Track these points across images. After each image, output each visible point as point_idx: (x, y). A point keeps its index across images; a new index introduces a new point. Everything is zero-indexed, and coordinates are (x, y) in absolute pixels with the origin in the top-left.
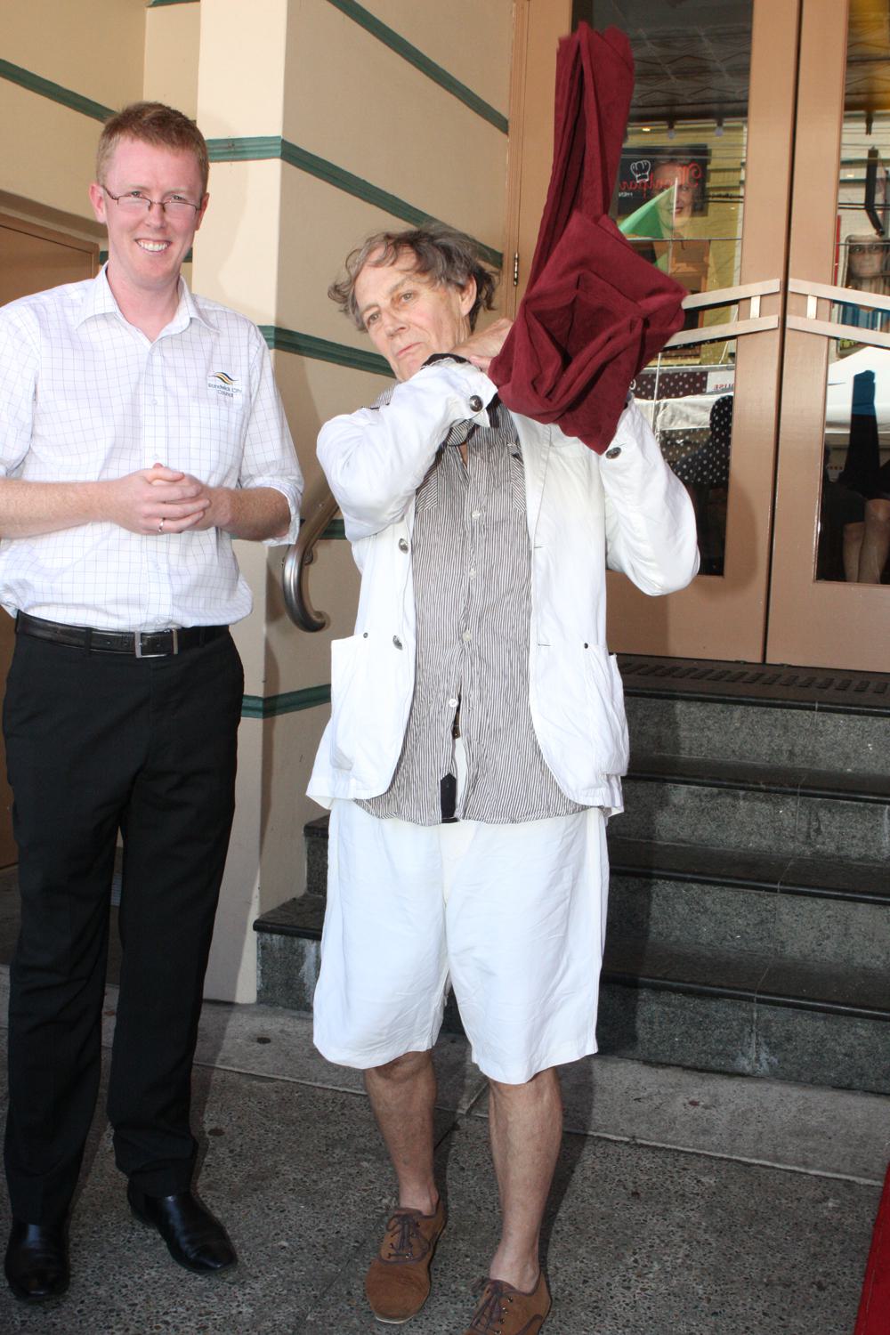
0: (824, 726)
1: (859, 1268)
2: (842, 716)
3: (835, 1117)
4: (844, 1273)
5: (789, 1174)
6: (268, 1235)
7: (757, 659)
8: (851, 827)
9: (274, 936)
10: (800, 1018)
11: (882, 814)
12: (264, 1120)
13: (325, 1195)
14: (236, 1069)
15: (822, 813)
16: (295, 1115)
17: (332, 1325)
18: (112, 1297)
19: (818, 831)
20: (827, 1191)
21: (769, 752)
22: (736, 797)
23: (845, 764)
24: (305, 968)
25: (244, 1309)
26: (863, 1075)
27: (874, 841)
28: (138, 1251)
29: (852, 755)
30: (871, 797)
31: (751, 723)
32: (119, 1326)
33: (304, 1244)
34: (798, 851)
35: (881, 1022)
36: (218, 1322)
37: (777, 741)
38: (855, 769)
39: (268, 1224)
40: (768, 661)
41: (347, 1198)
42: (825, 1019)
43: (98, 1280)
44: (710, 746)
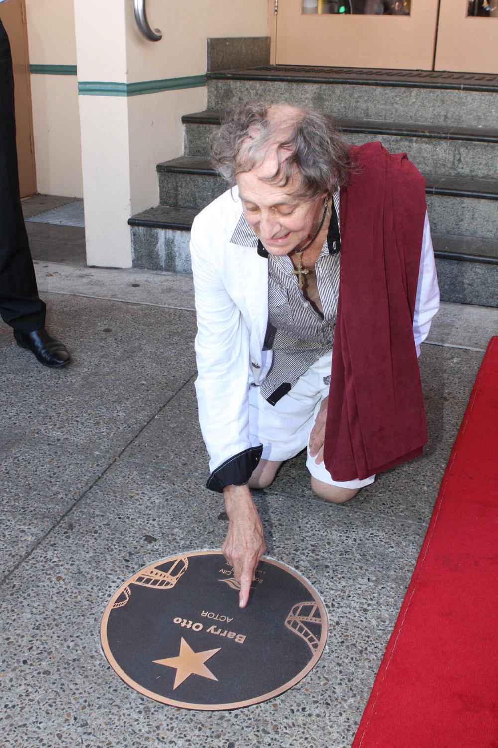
1: (468, 391)
2: (477, 93)
5: (432, 346)
7: (430, 69)
8: (479, 158)
9: (140, 228)
10: (443, 264)
12: (135, 324)
13: (168, 359)
14: (120, 300)
16: (152, 321)
17: (169, 420)
18: (47, 410)
19: (459, 160)
20: (453, 354)
21: (433, 117)
23: (478, 123)
24: (159, 245)
25: (120, 414)
26: (478, 296)
27: (492, 166)
29: (483, 117)
30: (492, 139)
31: (422, 99)
32: (51, 424)
33: (155, 382)
34: (447, 173)
36: (106, 420)
37: (438, 110)
38: (483, 126)
39: (135, 373)
40: (436, 69)
42: (458, 264)
43: (40, 402)
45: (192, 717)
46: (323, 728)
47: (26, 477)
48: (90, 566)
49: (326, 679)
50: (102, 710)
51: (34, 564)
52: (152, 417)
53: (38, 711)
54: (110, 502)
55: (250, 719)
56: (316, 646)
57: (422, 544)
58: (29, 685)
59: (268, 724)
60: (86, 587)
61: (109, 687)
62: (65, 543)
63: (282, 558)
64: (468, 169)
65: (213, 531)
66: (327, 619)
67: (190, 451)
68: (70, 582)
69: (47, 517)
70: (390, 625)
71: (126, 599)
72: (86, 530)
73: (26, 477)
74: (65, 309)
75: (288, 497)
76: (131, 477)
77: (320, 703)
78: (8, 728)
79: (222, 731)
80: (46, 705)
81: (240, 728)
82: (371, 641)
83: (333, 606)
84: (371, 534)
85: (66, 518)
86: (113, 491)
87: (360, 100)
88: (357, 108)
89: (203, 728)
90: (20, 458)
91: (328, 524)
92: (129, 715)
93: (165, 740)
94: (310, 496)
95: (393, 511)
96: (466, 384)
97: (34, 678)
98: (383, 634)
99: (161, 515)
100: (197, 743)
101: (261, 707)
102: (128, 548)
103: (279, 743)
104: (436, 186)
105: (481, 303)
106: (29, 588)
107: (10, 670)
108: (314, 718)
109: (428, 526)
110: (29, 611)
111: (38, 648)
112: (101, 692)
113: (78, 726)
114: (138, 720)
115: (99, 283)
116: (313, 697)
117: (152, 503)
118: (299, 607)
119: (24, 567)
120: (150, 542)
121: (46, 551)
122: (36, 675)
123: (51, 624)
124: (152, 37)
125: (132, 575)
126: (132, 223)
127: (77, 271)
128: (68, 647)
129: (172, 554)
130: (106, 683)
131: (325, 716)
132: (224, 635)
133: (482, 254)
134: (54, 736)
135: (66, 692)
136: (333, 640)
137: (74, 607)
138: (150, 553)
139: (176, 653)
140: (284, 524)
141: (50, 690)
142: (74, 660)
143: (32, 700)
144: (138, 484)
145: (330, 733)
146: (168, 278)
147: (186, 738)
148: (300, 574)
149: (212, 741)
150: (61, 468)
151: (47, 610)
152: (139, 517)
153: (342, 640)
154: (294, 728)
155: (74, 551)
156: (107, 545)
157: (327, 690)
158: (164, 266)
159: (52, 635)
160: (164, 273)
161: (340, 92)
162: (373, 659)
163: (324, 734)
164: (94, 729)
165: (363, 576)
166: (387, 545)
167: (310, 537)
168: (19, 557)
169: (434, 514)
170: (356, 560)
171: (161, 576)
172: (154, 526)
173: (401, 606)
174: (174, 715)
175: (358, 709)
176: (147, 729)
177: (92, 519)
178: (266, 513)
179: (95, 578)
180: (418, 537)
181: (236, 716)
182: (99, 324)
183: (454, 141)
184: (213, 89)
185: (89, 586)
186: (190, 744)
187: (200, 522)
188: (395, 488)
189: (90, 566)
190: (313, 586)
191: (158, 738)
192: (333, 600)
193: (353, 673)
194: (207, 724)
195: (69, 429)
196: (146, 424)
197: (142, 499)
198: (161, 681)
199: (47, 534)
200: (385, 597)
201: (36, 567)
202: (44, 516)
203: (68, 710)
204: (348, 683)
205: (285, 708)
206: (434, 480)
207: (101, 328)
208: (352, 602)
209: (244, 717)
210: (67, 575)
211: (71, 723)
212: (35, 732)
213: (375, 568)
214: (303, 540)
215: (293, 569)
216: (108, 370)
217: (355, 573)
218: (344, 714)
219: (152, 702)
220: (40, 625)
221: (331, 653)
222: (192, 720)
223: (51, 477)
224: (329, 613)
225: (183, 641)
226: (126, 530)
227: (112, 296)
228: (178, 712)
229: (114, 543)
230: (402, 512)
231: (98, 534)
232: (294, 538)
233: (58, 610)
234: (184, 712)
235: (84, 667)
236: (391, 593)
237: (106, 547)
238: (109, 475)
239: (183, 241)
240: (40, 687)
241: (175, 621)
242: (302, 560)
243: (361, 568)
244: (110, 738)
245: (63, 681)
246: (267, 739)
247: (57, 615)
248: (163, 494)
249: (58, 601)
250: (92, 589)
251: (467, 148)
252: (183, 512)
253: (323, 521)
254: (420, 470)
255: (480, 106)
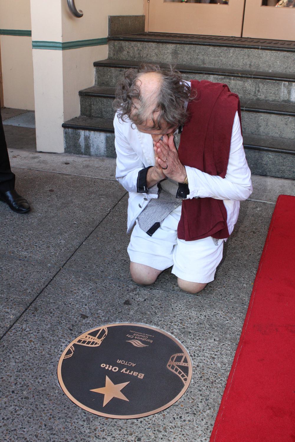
0: (262, 55)
1: (267, 228)
2: (269, 51)
3: (260, 184)
4: (262, 229)
6: (70, 220)
7: (240, 36)
9: (69, 129)
11: (281, 85)
13: (89, 208)
14: (58, 172)
15: (260, 85)
16: (78, 185)
17: (91, 245)
19: (259, 91)
20: (257, 205)
22: (230, 79)
23: (269, 69)
24: (80, 139)
26: (270, 171)
27: (278, 94)
28: (26, 226)
30: (278, 79)
31: (237, 54)
33: (82, 222)
34: (251, 98)
35: (278, 153)
36: (54, 245)
37: (246, 61)
38: (272, 71)
40: (243, 36)
41: (96, 209)
42: (258, 152)
44: (222, 63)
45: (115, 423)
46: (193, 428)
47: (7, 280)
48: (49, 333)
49: (193, 399)
50: (61, 420)
51: (15, 333)
52: (81, 243)
53: (23, 421)
54: (59, 295)
55: (150, 424)
56: (186, 380)
57: (245, 318)
58: (16, 406)
59: (160, 426)
60: (47, 346)
61: (65, 406)
62: (33, 320)
63: (163, 328)
64: (263, 96)
65: (121, 312)
66: (191, 364)
67: (105, 264)
68: (37, 343)
69: (22, 304)
70: (229, 367)
71: (72, 353)
72: (45, 312)
73: (7, 280)
74: (25, 178)
75: (164, 291)
76: (71, 279)
77: (190, 414)
78: (5, 432)
79: (133, 431)
80: (27, 418)
81: (144, 429)
82: (218, 376)
83: (194, 355)
84: (215, 313)
85: (33, 305)
86: (60, 288)
87: (200, 55)
88: (198, 59)
89: (122, 430)
90: (3, 268)
91: (189, 307)
92: (78, 423)
93: (100, 437)
94: (178, 290)
95: (227, 299)
96: (265, 223)
97: (19, 402)
98: (225, 372)
99: (90, 303)
100: (119, 439)
101: (155, 416)
102: (71, 322)
103: (167, 438)
104: (246, 106)
105: (272, 175)
106: (13, 347)
107: (4, 397)
108: (187, 422)
109: (248, 307)
110: (13, 361)
111: (21, 383)
112: (60, 409)
113: (47, 430)
114: (83, 426)
115: (44, 162)
116: (186, 410)
117: (84, 295)
118: (174, 357)
119: (9, 334)
120: (84, 318)
121: (22, 325)
122: (20, 399)
123: (27, 369)
124: (77, 15)
125: (74, 338)
126: (64, 126)
127: (31, 154)
128: (39, 382)
129: (98, 325)
130: (63, 404)
131: (193, 421)
132: (131, 374)
133: (273, 147)
134: (33, 436)
135: (39, 410)
136: (196, 376)
137: (41, 358)
138: (84, 325)
139: (104, 385)
140: (163, 307)
141: (29, 409)
142: (43, 390)
143: (18, 415)
144: (75, 283)
145: (197, 431)
146: (86, 159)
147: (112, 436)
148: (174, 337)
149: (128, 437)
150: (28, 274)
151: (24, 360)
152: (77, 304)
153: (201, 376)
154: (175, 429)
155: (39, 324)
156: (59, 320)
157: (193, 406)
158: (83, 152)
159: (28, 375)
160: (84, 156)
161: (188, 49)
162: (220, 387)
163: (193, 432)
164: (57, 431)
165: (211, 338)
166: (224, 319)
167: (179, 315)
168: (6, 328)
169: (251, 300)
170: (207, 329)
171: (92, 338)
172: (86, 309)
173: (234, 355)
174: (104, 422)
175: (212, 416)
176: (89, 431)
177: (49, 305)
178: (152, 301)
179: (52, 341)
180: (242, 314)
181: (141, 422)
182: (46, 187)
183: (255, 79)
184: (112, 46)
185: (49, 345)
186: (115, 440)
187: (113, 306)
188: (227, 285)
189: (49, 333)
190: (182, 344)
191: (95, 436)
192: (195, 352)
193: (208, 396)
194: (124, 427)
195: (31, 250)
196: (78, 247)
197: (77, 292)
198: (96, 402)
199: (22, 315)
200: (225, 350)
201: (16, 334)
202: (19, 303)
203: (41, 420)
204: (206, 401)
205: (170, 417)
206: (250, 281)
207: (47, 189)
208: (206, 353)
209: (146, 423)
210: (35, 339)
211: (43, 428)
212: (21, 434)
213: (218, 333)
214: (175, 317)
215: (170, 334)
216: (53, 215)
217: (206, 336)
218: (204, 420)
219: (91, 415)
220: (21, 369)
221: (195, 383)
222: (115, 425)
223: (22, 280)
224: (193, 360)
225: (107, 378)
226: (69, 311)
227: (53, 170)
228: (107, 421)
229: (63, 319)
230: (232, 299)
231: (52, 314)
232: (169, 316)
233: (31, 360)
234: (110, 420)
235: (49, 394)
236: (228, 348)
237: (58, 322)
238: (58, 278)
239: (95, 137)
240: (23, 407)
241: (102, 366)
242: (175, 328)
243: (210, 333)
244: (67, 437)
245: (37, 403)
246: (160, 436)
247: (31, 363)
248: (90, 290)
249: (31, 355)
250: (51, 347)
251: (263, 84)
252: (103, 300)
253: (186, 305)
254: (241, 275)
255: (270, 59)
